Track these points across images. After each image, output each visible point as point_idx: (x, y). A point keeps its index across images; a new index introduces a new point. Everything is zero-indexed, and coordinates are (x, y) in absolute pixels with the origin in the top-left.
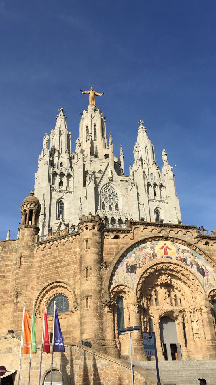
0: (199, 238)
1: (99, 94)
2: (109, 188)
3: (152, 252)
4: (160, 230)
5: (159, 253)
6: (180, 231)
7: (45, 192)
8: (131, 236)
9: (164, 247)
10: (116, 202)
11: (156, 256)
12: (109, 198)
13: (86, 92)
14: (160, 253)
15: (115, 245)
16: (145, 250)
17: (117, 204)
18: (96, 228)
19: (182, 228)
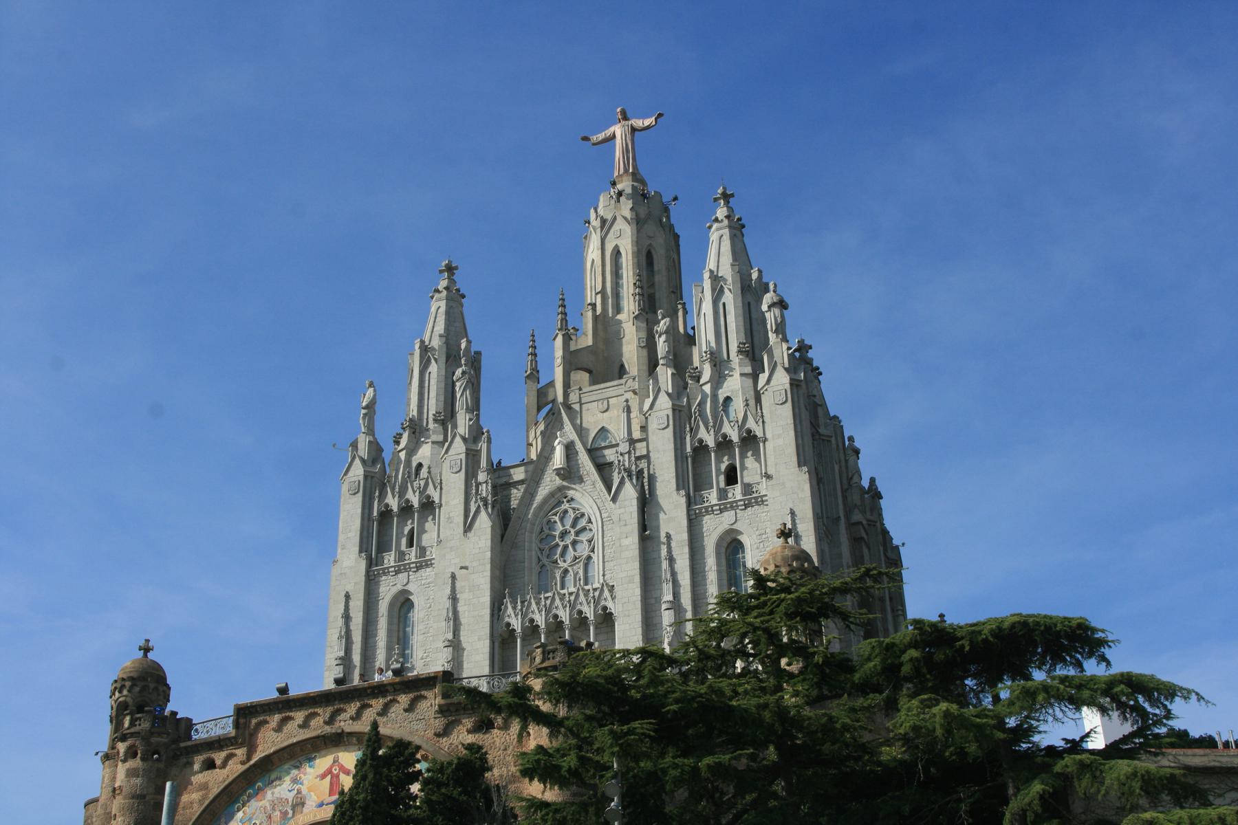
0: (448, 710)
1: (647, 122)
2: (565, 506)
3: (296, 791)
4: (328, 715)
5: (312, 793)
6: (391, 701)
7: (349, 588)
8: (241, 752)
9: (333, 770)
10: (586, 553)
11: (303, 804)
12: (561, 544)
13: (601, 136)
14: (315, 795)
15: (201, 790)
16: (273, 793)
17: (589, 558)
18: (139, 755)
19: (395, 690)
